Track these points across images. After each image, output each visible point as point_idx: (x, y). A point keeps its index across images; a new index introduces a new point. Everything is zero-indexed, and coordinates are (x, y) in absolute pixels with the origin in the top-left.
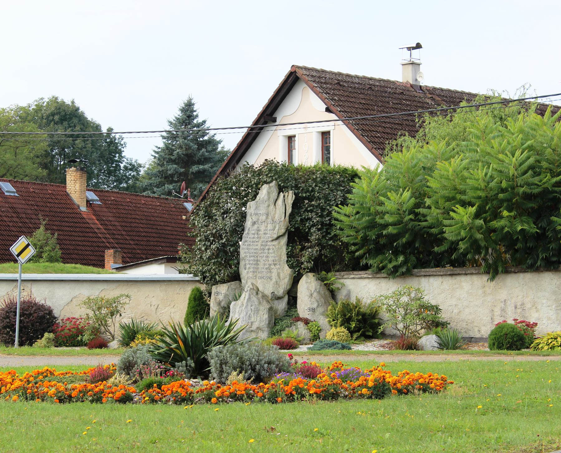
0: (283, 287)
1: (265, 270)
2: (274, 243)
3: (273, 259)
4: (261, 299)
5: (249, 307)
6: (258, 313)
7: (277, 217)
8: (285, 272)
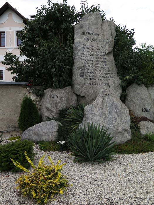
1: (102, 78)
2: (106, 57)
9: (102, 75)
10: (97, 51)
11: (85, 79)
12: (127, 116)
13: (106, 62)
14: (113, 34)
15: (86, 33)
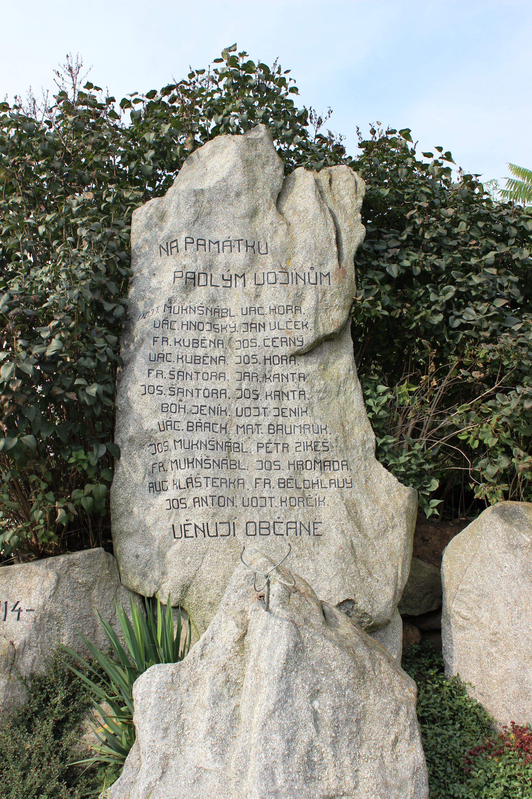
0: (390, 571)
1: (277, 492)
3: (311, 437)
4: (361, 651)
5: (300, 701)
6: (357, 738)
7: (300, 261)
8: (384, 499)
9: (275, 476)
10: (250, 335)
11: (176, 504)
12: (396, 741)
13: (302, 393)
14: (344, 236)
15: (181, 244)
